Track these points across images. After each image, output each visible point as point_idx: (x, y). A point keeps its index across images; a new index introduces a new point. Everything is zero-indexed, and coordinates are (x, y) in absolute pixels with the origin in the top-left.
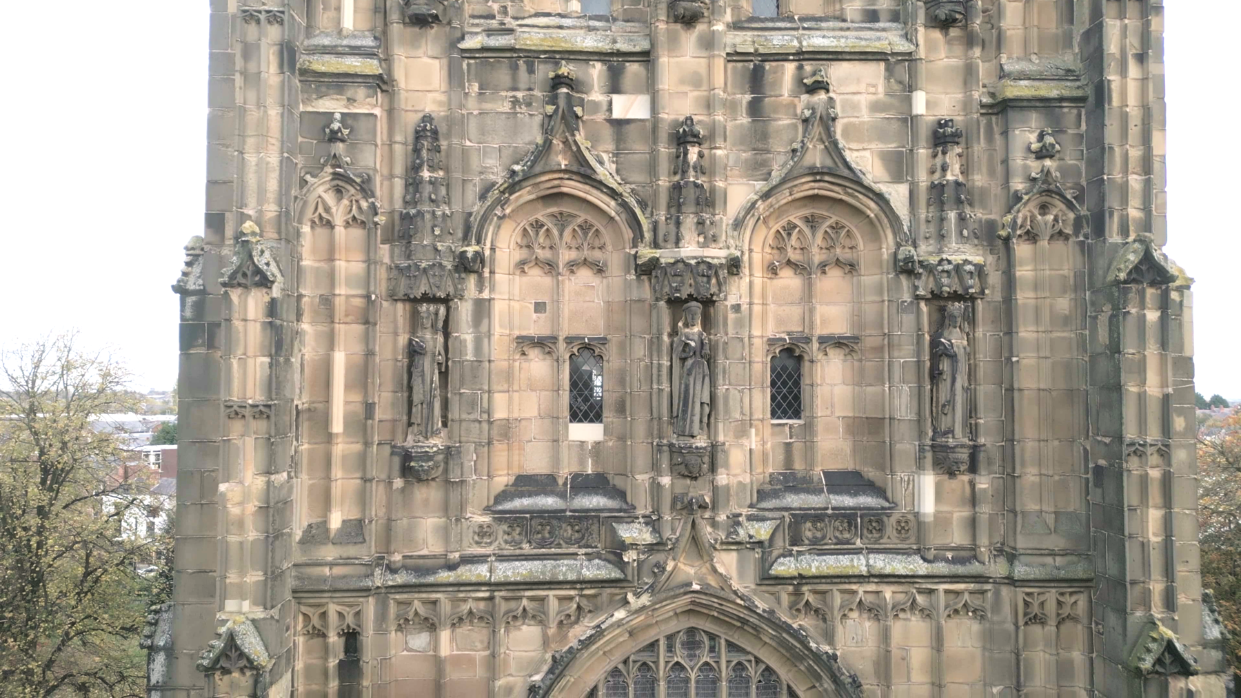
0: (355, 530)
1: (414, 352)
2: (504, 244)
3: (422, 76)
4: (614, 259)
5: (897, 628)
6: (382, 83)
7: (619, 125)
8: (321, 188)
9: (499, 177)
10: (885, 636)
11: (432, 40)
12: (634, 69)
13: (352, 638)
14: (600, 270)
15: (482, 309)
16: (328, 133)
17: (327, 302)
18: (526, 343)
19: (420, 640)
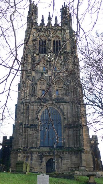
0: (29, 99)
1: (33, 89)
2: (38, 83)
3: (33, 73)
4: (46, 84)
5: (64, 106)
6: (31, 74)
7: (46, 76)
8: (27, 79)
9: (38, 79)
10: (64, 106)
11: (34, 71)
12: (47, 73)
13: (28, 106)
14: (44, 85)
15: (37, 87)
16: (28, 76)
17: (27, 86)
18: (39, 90)
19: (33, 107)
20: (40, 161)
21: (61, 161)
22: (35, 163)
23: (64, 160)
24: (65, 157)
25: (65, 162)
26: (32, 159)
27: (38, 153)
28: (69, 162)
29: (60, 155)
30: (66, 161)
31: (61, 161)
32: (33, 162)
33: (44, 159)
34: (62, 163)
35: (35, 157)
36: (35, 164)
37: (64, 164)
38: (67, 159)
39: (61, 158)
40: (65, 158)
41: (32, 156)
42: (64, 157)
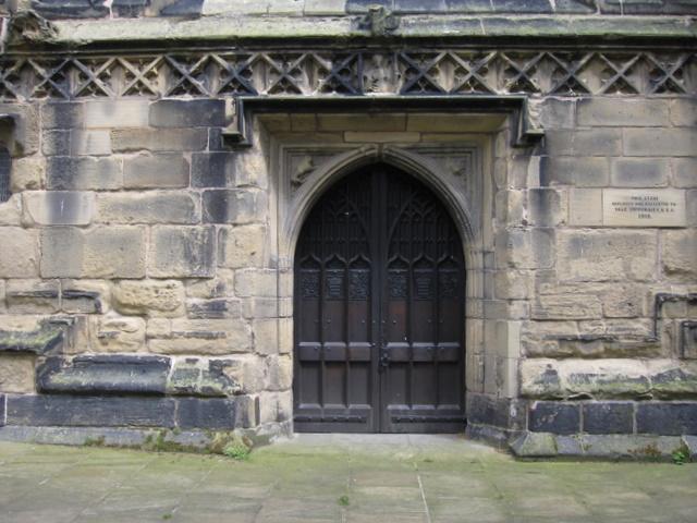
20: (196, 196)
21: (542, 199)
22: (120, 227)
23: (595, 179)
24: (605, 144)
25: (598, 206)
26: (64, 170)
27: (161, 85)
28: (658, 219)
29: (516, 106)
30: (611, 196)
31: (542, 199)
32: (89, 206)
33: (253, 166)
34: (545, 232)
35: (125, 140)
36: (125, 243)
37: (577, 245)
38: (629, 174)
39: (532, 143)
40: (598, 161)
41: (65, 125)
42: (585, 134)
